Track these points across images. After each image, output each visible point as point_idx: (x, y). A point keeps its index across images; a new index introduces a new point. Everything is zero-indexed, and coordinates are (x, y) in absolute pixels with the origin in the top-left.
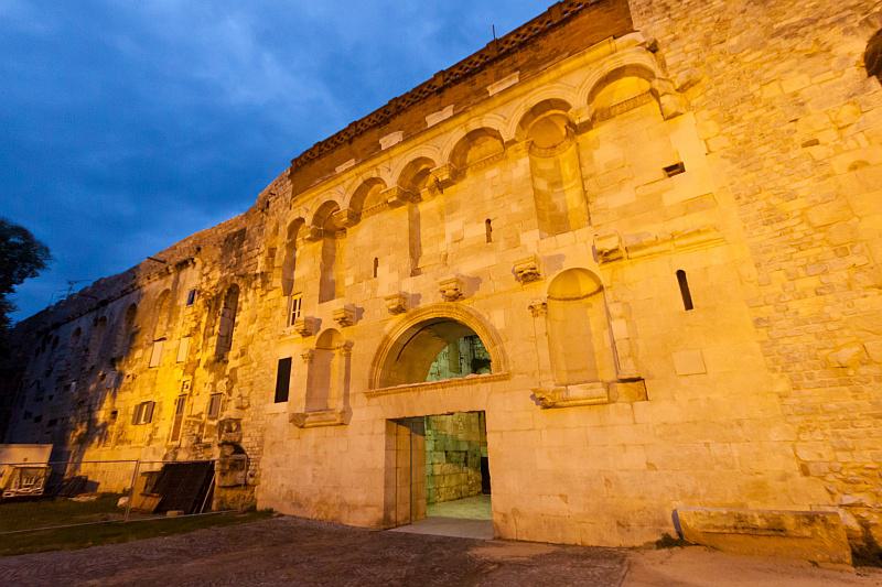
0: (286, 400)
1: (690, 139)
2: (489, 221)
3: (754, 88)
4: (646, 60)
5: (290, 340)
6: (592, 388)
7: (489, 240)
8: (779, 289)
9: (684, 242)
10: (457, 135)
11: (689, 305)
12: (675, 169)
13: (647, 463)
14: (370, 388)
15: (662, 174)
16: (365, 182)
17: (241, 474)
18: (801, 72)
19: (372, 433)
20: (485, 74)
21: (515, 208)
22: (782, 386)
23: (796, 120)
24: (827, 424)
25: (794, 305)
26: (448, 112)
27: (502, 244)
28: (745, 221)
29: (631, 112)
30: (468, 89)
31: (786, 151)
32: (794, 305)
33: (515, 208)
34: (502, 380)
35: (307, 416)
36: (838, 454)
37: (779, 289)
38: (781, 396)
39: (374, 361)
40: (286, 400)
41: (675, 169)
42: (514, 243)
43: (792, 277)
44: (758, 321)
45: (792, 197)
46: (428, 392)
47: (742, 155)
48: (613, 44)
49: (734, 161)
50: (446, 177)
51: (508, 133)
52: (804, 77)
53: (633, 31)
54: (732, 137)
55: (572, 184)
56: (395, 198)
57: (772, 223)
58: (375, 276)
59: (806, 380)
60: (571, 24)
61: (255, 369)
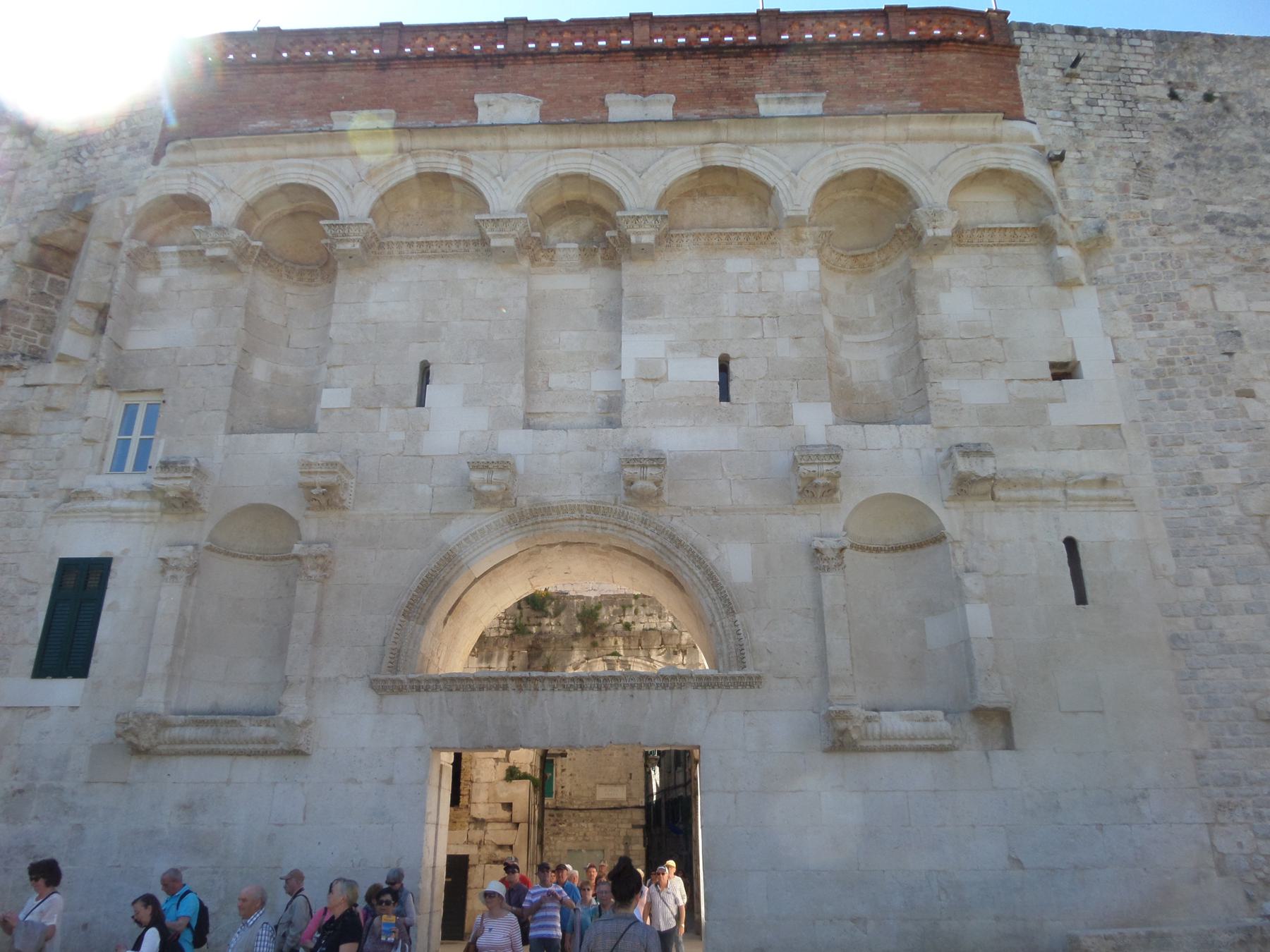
0: (81, 671)
4: (1041, 173)
5: (110, 510)
6: (927, 720)
7: (725, 395)
8: (1200, 593)
9: (1081, 492)
11: (1081, 598)
12: (1064, 371)
13: (1010, 857)
14: (394, 668)
15: (1047, 373)
16: (420, 176)
18: (1238, 287)
19: (390, 781)
20: (751, 67)
21: (785, 349)
23: (1230, 354)
24: (1250, 801)
25: (1220, 622)
26: (662, 107)
29: (1004, 250)
30: (710, 77)
31: (1216, 393)
32: (1220, 622)
33: (785, 349)
34: (744, 686)
36: (1261, 843)
37: (1200, 593)
38: (1199, 757)
39: (410, 605)
41: (1064, 371)
42: (780, 418)
43: (1218, 580)
45: (1221, 463)
46: (559, 694)
48: (998, 127)
49: (1151, 385)
50: (648, 239)
52: (1241, 295)
53: (1022, 118)
56: (510, 242)
57: (1197, 494)
58: (421, 402)
59: (1228, 736)
60: (926, 56)
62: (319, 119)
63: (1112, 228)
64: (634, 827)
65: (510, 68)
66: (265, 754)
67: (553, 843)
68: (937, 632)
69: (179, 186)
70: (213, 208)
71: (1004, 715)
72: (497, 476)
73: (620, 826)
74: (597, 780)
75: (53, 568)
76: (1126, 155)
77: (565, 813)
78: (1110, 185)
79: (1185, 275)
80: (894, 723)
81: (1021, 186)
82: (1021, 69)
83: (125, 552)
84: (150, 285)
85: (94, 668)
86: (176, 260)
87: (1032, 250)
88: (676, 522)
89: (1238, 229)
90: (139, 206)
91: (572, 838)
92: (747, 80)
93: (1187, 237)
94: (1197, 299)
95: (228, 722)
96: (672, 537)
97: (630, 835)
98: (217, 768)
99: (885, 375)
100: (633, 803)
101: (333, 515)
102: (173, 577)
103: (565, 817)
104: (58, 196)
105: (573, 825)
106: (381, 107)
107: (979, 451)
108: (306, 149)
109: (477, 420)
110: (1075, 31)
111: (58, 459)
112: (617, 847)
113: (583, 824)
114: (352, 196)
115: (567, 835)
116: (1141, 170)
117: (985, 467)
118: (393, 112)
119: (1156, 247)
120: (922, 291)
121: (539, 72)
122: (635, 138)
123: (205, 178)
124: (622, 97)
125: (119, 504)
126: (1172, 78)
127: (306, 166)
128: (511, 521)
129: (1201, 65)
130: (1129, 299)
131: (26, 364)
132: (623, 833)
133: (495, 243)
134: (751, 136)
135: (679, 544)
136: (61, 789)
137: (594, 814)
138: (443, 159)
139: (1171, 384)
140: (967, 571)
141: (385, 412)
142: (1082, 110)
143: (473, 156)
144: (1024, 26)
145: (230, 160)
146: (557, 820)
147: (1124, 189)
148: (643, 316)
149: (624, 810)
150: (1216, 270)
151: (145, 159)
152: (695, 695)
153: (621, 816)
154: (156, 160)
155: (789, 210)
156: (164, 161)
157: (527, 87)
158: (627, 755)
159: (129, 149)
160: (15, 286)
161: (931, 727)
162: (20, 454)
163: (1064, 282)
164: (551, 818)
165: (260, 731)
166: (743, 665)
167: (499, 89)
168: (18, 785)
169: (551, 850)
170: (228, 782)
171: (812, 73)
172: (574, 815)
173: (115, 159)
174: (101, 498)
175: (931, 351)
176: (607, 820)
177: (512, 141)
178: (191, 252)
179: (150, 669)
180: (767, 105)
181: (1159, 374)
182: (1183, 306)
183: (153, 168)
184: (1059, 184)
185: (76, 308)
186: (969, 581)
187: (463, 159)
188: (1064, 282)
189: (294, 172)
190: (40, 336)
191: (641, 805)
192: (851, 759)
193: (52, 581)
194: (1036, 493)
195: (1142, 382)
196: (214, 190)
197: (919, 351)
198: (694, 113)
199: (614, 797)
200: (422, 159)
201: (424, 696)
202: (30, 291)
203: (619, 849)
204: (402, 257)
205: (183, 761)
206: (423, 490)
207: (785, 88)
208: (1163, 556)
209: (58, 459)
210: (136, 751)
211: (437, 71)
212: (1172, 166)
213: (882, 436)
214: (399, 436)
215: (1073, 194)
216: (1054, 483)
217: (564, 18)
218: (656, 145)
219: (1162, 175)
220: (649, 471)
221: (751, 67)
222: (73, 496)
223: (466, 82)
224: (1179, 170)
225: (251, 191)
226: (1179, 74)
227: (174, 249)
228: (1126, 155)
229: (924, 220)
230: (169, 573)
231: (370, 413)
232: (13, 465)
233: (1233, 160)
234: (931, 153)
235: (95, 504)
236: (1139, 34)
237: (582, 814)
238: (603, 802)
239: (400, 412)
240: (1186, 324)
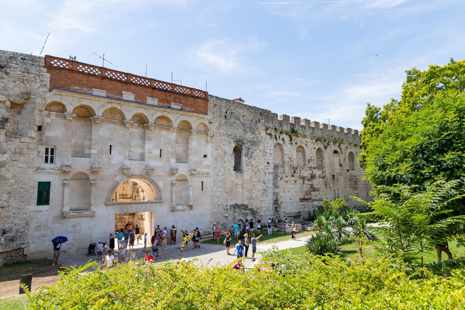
0: (49, 204)
1: (209, 149)
2: (161, 150)
3: (221, 145)
5: (49, 172)
7: (160, 157)
9: (205, 175)
10: (159, 114)
11: (202, 190)
17: (15, 244)
20: (170, 95)
21: (170, 149)
22: (212, 208)
25: (216, 193)
27: (164, 160)
28: (214, 174)
35: (70, 213)
40: (49, 204)
42: (168, 161)
44: (211, 195)
45: (221, 172)
46: (135, 205)
47: (216, 159)
51: (176, 124)
54: (216, 153)
55: (181, 145)
58: (110, 153)
60: (197, 100)
61: (13, 185)
62: (90, 89)
63: (215, 134)
65: (129, 85)
66: (87, 217)
68: (184, 193)
69: (57, 99)
70: (67, 107)
71: (192, 206)
72: (128, 171)
75: (37, 184)
76: (219, 122)
78: (216, 127)
79: (222, 143)
80: (179, 207)
81: (205, 125)
82: (209, 104)
83: (53, 181)
84: (48, 120)
85: (50, 203)
86: (55, 115)
87: (204, 136)
88: (153, 178)
89: (229, 136)
90: (48, 103)
92: (170, 98)
93: (223, 137)
94: (222, 147)
95: (81, 212)
96: (152, 180)
98: (79, 219)
99: (181, 152)
101: (96, 175)
102: (67, 186)
104: (18, 92)
106: (103, 89)
107: (195, 170)
108: (88, 98)
109: (121, 158)
110: (216, 97)
111: (33, 160)
114: (99, 111)
116: (220, 125)
117: (195, 173)
118: (106, 91)
119: (219, 138)
120: (190, 141)
121: (133, 87)
122: (152, 108)
123: (65, 100)
124: (149, 98)
125: (50, 171)
126: (227, 108)
127: (89, 102)
128: (127, 177)
129: (230, 106)
130: (215, 146)
131: (20, 137)
133: (127, 125)
134: (170, 111)
135: (153, 181)
136: (48, 225)
138: (117, 105)
139: (217, 160)
140: (190, 186)
141: (104, 155)
142: (215, 113)
143: (123, 107)
144: (210, 95)
145: (70, 96)
147: (217, 128)
148: (149, 141)
150: (226, 143)
151: (46, 90)
152: (154, 204)
154: (50, 90)
155: (174, 127)
156: (52, 92)
157: (132, 91)
159: (41, 85)
160: (8, 113)
161: (184, 208)
162: (22, 158)
163: (207, 142)
165: (87, 213)
166: (161, 200)
167: (127, 90)
168: (38, 225)
170: (81, 221)
171: (180, 99)
173: (37, 87)
174: (46, 169)
175: (189, 151)
177: (130, 104)
178: (59, 114)
179: (65, 203)
180: (173, 105)
181: (216, 158)
182: (221, 148)
183: (49, 93)
184: (210, 126)
185: (34, 126)
186: (190, 188)
187: (121, 106)
188: (207, 142)
189: (86, 102)
190: (14, 125)
192: (174, 212)
193: (37, 186)
194: (200, 175)
195: (214, 159)
196: (67, 103)
197: (188, 151)
198: (161, 104)
200: (113, 105)
201: (114, 206)
202: (10, 114)
204: (106, 123)
205: (72, 219)
206: (112, 170)
207: (176, 102)
208: (212, 184)
209: (33, 160)
210: (64, 218)
211: (114, 82)
212: (224, 125)
213: (182, 165)
214: (107, 160)
215: (211, 128)
216: (202, 174)
217: (138, 75)
218: (155, 110)
219: (222, 126)
220: (152, 171)
221: (170, 95)
222: (38, 169)
223: (120, 87)
224: (224, 126)
225: (77, 104)
226: (228, 108)
227: (55, 113)
228: (219, 122)
229: (193, 131)
230: (66, 186)
231: (101, 155)
232: (21, 161)
233: (231, 124)
234: (195, 119)
235: (46, 171)
236: (224, 99)
239: (107, 155)
240: (221, 151)
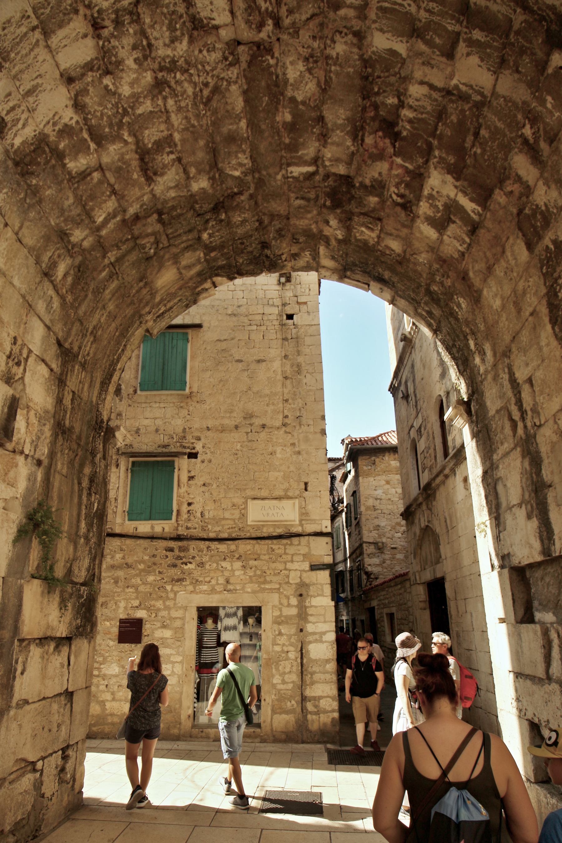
64: (314, 568)
67: (171, 595)
73: (289, 565)
74: (249, 493)
77: (193, 544)
91: (205, 587)
97: (307, 581)
100: (310, 528)
103: (192, 552)
105: (207, 567)
112: (285, 602)
113: (224, 564)
115: (196, 582)
132: (294, 578)
137: (244, 547)
146: (179, 558)
149: (295, 540)
153: (291, 550)
158: (299, 453)
164: (168, 553)
169: (168, 608)
172: (208, 547)
176: (267, 557)
191: (325, 530)
199: (281, 518)
203: (289, 605)
237: (223, 547)
238: (259, 528)
